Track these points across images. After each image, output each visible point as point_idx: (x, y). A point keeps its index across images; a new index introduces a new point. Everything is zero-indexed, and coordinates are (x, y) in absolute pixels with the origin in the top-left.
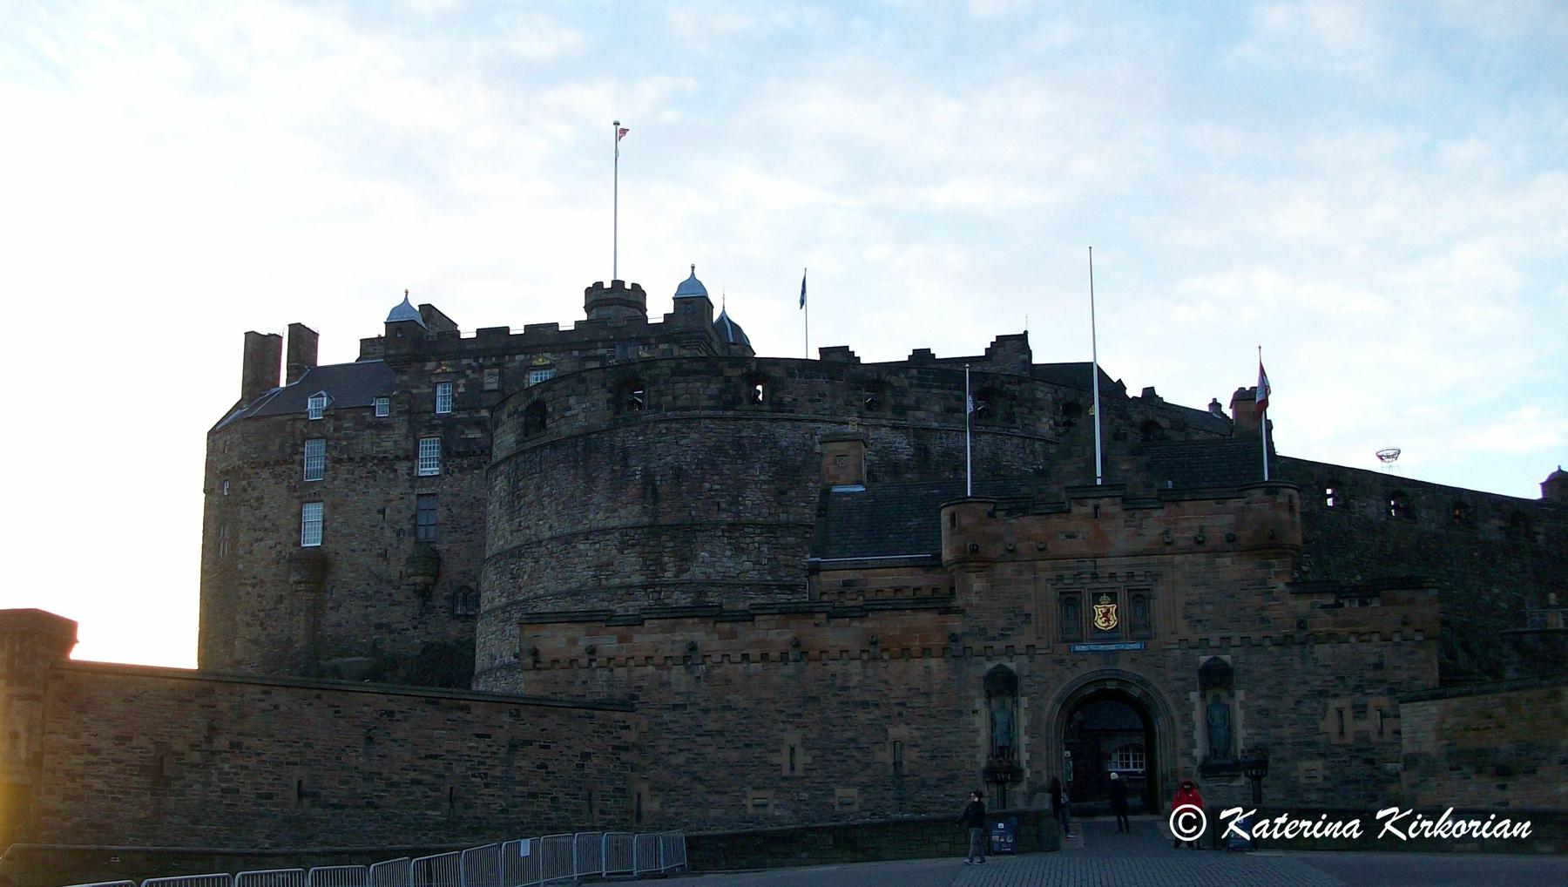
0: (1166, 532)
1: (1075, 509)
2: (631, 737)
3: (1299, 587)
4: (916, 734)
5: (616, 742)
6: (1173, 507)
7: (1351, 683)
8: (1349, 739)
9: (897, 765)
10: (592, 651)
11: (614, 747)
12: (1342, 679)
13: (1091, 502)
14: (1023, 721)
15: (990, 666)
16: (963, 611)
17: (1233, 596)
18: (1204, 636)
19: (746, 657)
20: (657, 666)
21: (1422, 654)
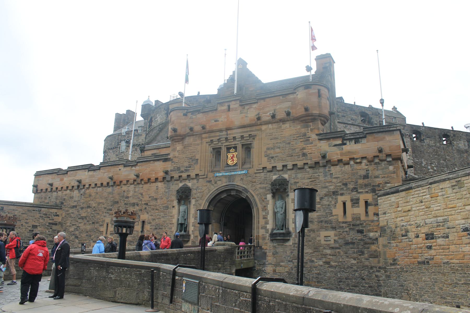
0: (259, 114)
1: (220, 108)
2: (58, 219)
3: (323, 137)
4: (150, 217)
5: (51, 221)
6: (262, 101)
7: (351, 186)
8: (349, 218)
9: (142, 231)
10: (51, 185)
11: (50, 223)
12: (345, 184)
13: (227, 104)
14: (193, 211)
15: (181, 185)
16: (172, 160)
17: (289, 143)
18: (274, 165)
19: (96, 184)
20: (70, 190)
21: (391, 168)
